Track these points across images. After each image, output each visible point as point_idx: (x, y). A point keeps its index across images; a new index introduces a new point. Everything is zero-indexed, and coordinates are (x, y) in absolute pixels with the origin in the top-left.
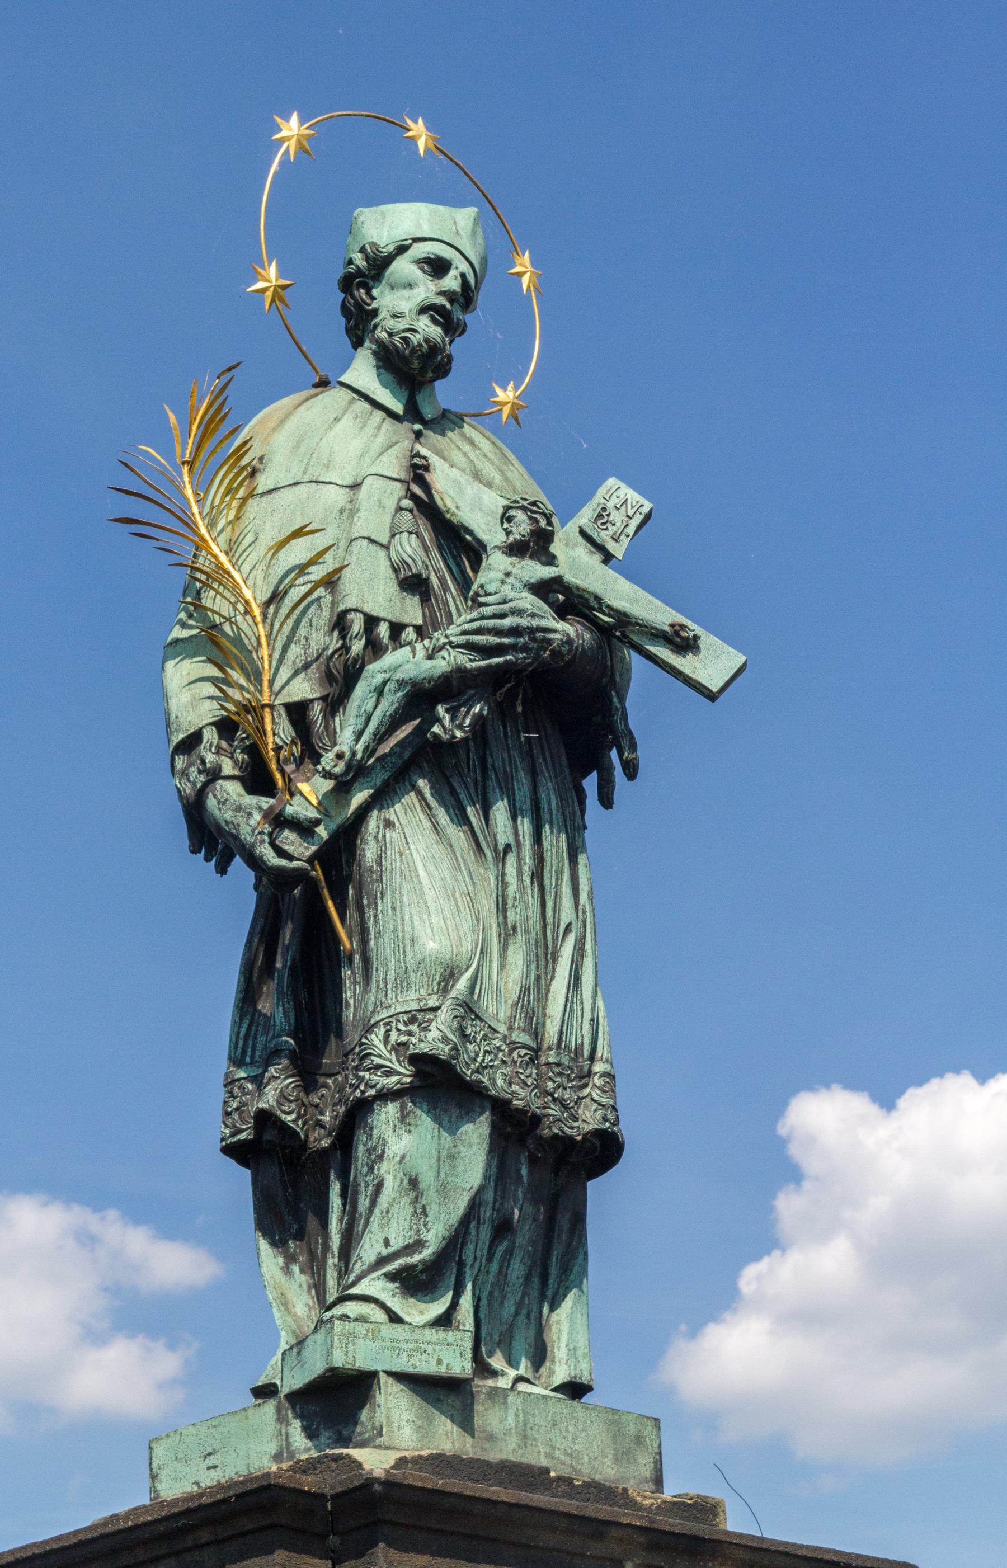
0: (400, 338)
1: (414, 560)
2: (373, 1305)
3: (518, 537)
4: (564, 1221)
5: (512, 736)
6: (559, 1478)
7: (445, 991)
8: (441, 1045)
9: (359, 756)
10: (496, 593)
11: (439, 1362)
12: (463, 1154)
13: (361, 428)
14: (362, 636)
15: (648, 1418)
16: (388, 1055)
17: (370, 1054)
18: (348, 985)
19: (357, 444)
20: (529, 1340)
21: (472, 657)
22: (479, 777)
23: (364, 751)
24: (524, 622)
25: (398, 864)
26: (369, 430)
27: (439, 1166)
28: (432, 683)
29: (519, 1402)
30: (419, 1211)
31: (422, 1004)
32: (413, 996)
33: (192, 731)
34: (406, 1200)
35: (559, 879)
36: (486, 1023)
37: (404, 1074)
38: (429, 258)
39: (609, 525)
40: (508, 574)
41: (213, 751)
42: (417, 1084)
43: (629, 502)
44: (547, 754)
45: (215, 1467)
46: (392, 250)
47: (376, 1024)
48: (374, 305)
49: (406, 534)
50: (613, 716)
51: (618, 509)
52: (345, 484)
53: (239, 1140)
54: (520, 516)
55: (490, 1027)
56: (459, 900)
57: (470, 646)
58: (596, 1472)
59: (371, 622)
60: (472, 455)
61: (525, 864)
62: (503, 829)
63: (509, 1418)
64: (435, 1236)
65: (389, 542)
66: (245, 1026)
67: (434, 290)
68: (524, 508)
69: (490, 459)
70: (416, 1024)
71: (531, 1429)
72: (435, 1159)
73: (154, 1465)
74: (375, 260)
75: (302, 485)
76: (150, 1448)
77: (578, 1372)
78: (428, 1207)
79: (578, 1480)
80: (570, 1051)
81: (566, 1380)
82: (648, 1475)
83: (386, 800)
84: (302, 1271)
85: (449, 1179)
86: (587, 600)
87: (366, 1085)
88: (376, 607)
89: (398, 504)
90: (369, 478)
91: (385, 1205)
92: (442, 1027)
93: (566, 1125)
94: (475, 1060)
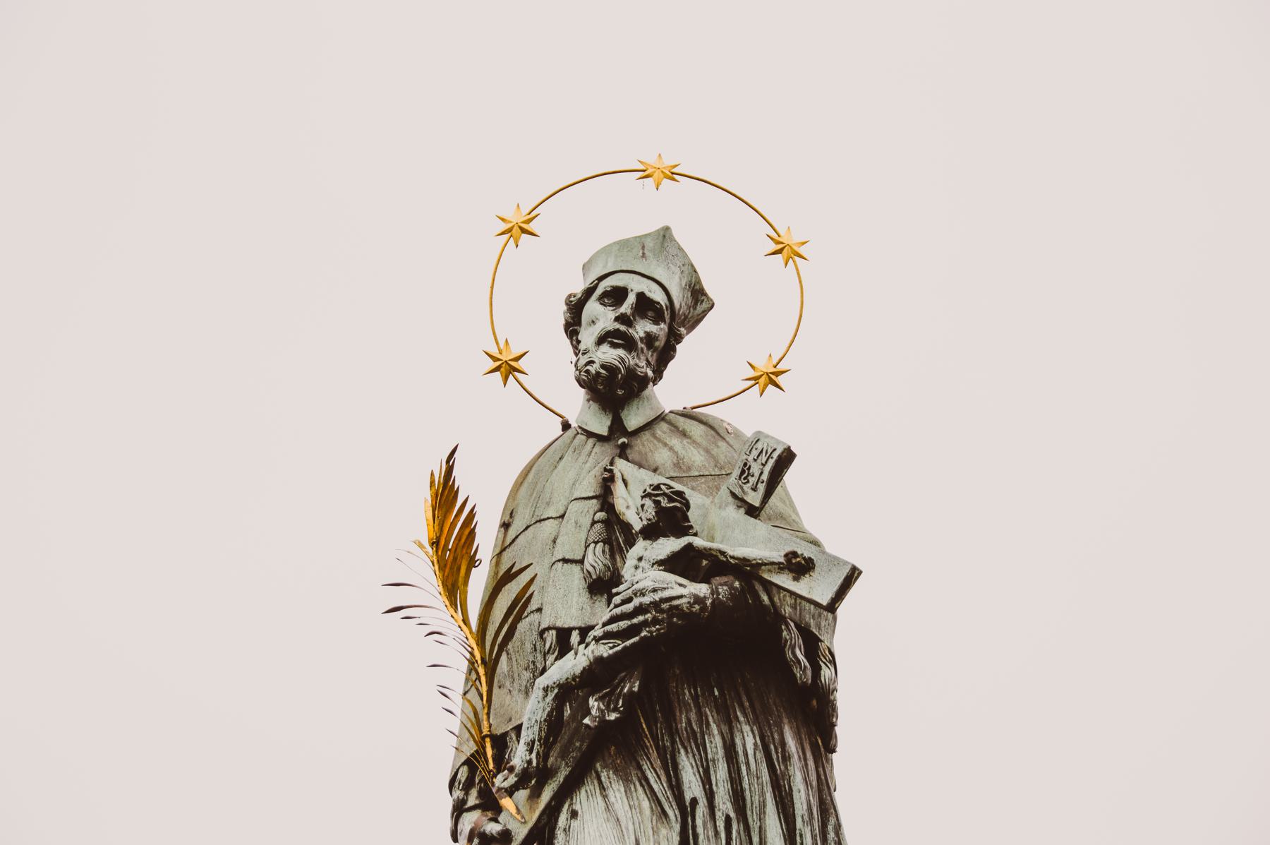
1: (594, 567)
5: (703, 694)
9: (534, 764)
13: (577, 459)
21: (611, 645)
23: (537, 758)
24: (647, 600)
28: (577, 680)
40: (640, 559)
41: (460, 788)
44: (744, 698)
51: (755, 460)
54: (648, 503)
57: (608, 636)
62: (688, 785)
75: (531, 527)
83: (576, 793)
86: (716, 556)
88: (569, 620)
89: (593, 519)
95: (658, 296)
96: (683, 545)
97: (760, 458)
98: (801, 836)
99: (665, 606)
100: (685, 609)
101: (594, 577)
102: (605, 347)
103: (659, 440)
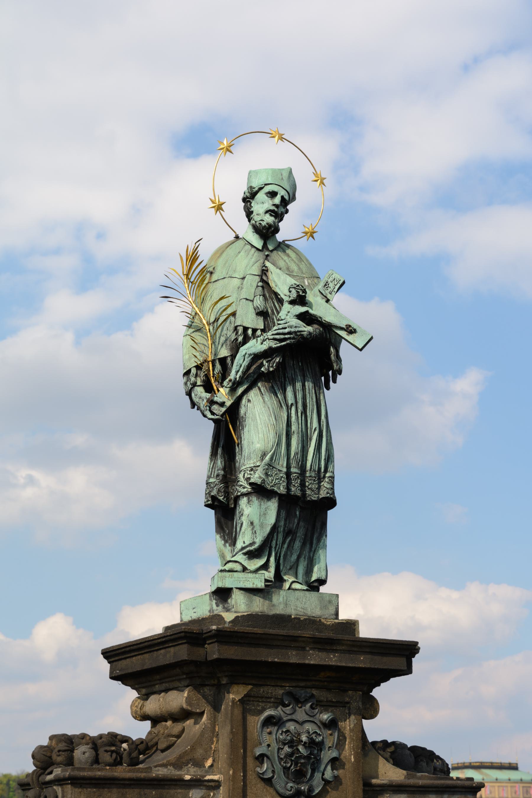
0: (259, 223)
1: (260, 306)
2: (237, 564)
3: (292, 298)
4: (318, 525)
5: (296, 364)
6: (295, 618)
7: (262, 460)
8: (258, 479)
9: (238, 379)
10: (284, 319)
11: (253, 584)
12: (268, 513)
13: (247, 255)
14: (242, 335)
15: (334, 594)
16: (243, 481)
17: (239, 481)
18: (237, 455)
19: (245, 262)
20: (304, 566)
22: (283, 381)
23: (239, 378)
25: (251, 415)
26: (250, 256)
27: (260, 518)
29: (284, 593)
30: (254, 532)
31: (255, 465)
32: (252, 462)
33: (188, 369)
34: (250, 529)
35: (312, 412)
36: (277, 469)
37: (249, 489)
38: (269, 192)
39: (328, 288)
40: (289, 312)
42: (253, 491)
43: (336, 279)
44: (309, 368)
45: (195, 612)
46: (257, 189)
47: (241, 471)
48: (252, 209)
49: (259, 296)
50: (331, 355)
51: (332, 282)
52: (240, 278)
53: (208, 504)
54: (293, 291)
55: (279, 470)
56: (270, 427)
58: (313, 613)
59: (245, 329)
60: (287, 261)
61: (299, 409)
63: (281, 599)
64: (258, 541)
65: (254, 299)
66: (212, 464)
67: (272, 203)
68: (294, 288)
69: (294, 261)
70: (253, 471)
71: (289, 601)
72: (259, 515)
73: (181, 610)
74: (251, 193)
76: (180, 604)
77: (321, 576)
78: (256, 531)
79: (302, 618)
80: (315, 471)
81: (316, 579)
82: (333, 613)
84: (230, 546)
85: (264, 522)
86: (317, 318)
87: (238, 491)
89: (257, 284)
90: (248, 275)
91: (243, 531)
92: (259, 473)
93: (313, 497)
94: (272, 482)
95: (287, 197)
96: (305, 310)
97: (334, 281)
98: (323, 422)
99: (298, 333)
100: (305, 336)
101: (261, 310)
102: (268, 215)
103: (280, 256)
